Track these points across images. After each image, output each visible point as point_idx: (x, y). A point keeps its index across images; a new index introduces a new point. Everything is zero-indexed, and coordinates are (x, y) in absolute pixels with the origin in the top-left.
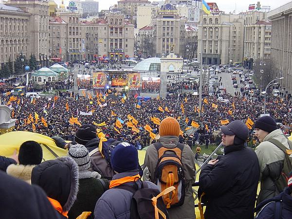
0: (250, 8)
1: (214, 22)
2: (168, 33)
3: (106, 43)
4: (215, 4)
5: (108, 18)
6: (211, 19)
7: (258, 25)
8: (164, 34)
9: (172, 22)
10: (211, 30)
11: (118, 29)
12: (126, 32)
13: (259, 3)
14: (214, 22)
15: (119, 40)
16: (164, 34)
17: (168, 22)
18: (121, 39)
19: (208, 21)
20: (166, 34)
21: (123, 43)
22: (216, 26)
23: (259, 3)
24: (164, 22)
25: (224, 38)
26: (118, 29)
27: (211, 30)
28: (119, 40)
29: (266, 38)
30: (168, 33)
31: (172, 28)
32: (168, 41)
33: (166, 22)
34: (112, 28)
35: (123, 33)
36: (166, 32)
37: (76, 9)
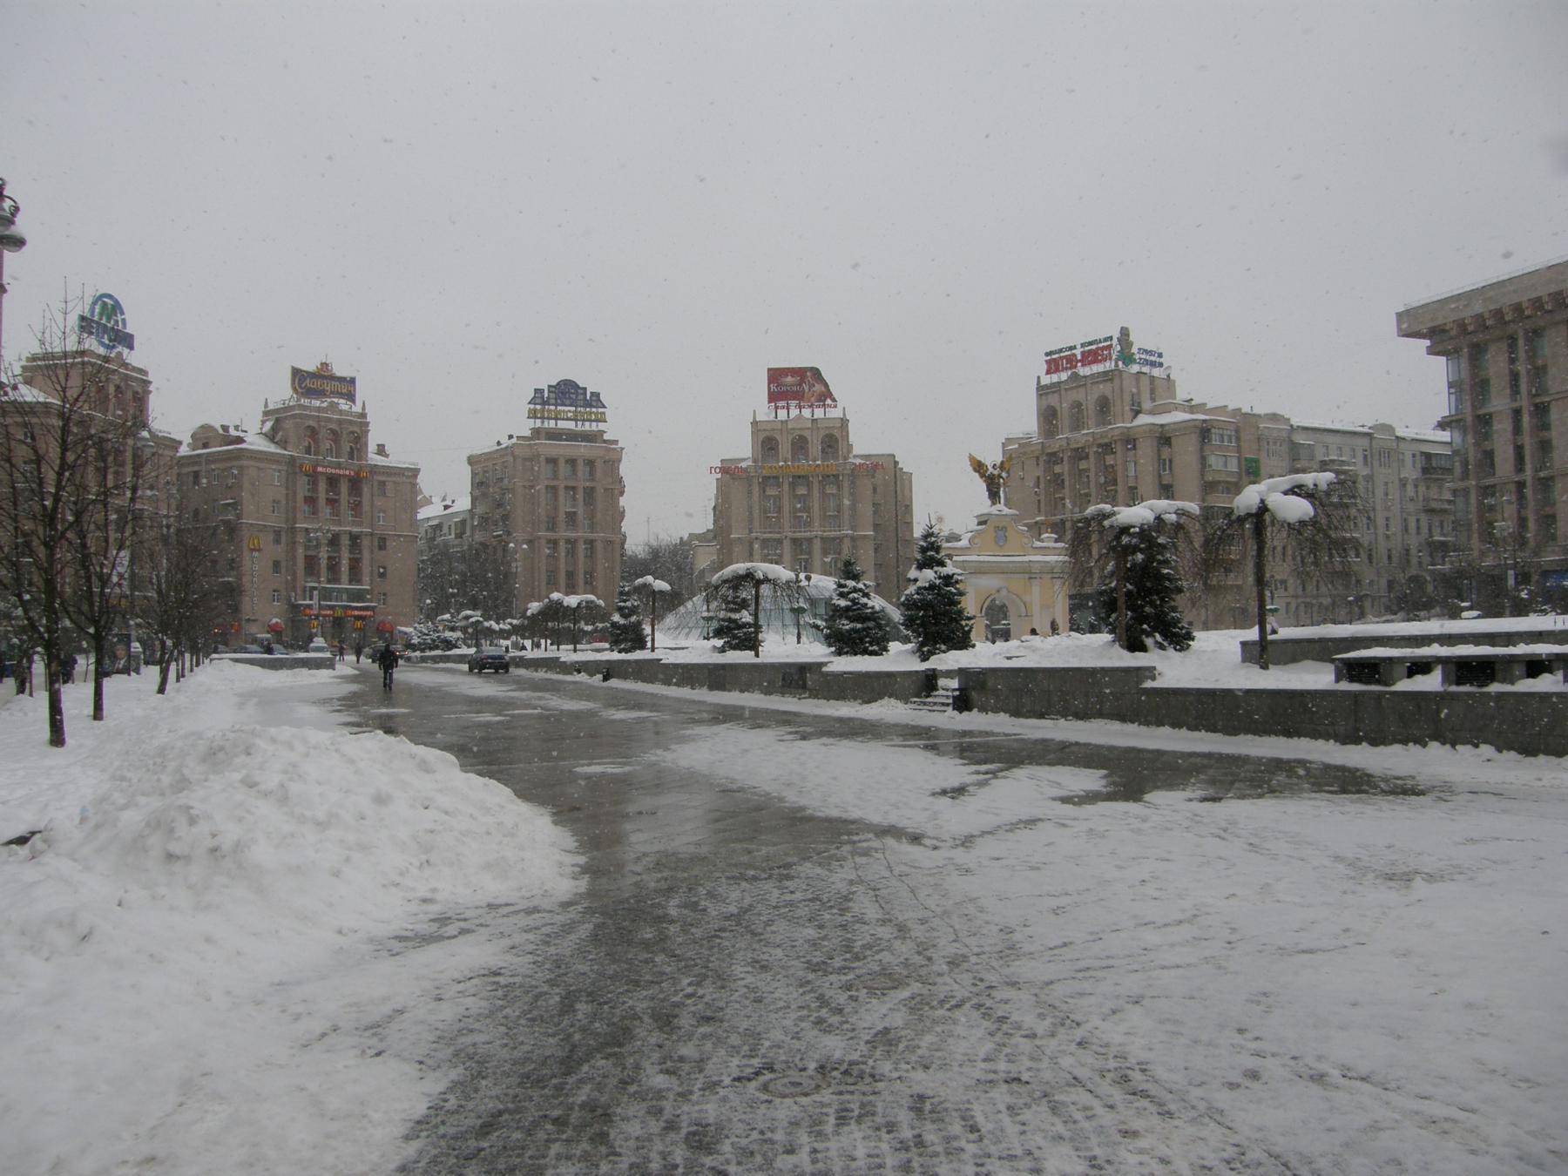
0: (1053, 366)
1: (815, 448)
2: (571, 517)
3: (279, 551)
4: (816, 372)
5: (288, 425)
6: (800, 445)
11: (344, 488)
12: (379, 502)
13: (1125, 332)
15: (345, 541)
18: (355, 539)
19: (785, 448)
20: (562, 517)
21: (366, 555)
23: (1125, 332)
24: (552, 461)
26: (344, 488)
27: (802, 491)
28: (345, 541)
30: (571, 517)
32: (572, 552)
33: (562, 463)
34: (313, 477)
35: (366, 506)
36: (565, 506)
37: (128, 341)
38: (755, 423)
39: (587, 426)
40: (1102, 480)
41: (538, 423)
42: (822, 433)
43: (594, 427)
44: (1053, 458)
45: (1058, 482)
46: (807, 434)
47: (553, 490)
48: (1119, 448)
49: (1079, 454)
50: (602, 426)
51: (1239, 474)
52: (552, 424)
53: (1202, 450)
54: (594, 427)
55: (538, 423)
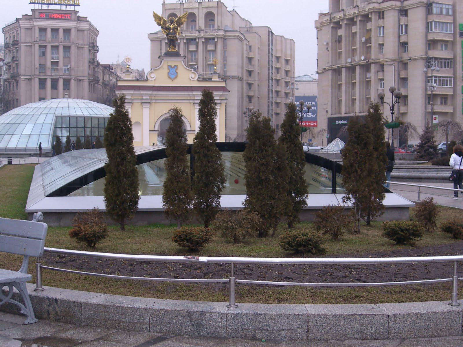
1: (200, 22)
2: (55, 64)
7: (398, 4)
8: (42, 67)
9: (67, 31)
10: (192, 48)
14: (200, 22)
16: (42, 67)
17: (55, 30)
20: (49, 65)
22: (211, 34)
24: (43, 30)
25: (234, 70)
29: (432, 44)
30: (55, 64)
31: (67, 49)
38: (164, 5)
39: (68, 8)
40: (363, 40)
41: (37, 7)
42: (205, 11)
43: (72, 8)
44: (337, 25)
45: (339, 40)
46: (196, 12)
47: (43, 47)
48: (373, 17)
49: (352, 21)
50: (77, 8)
51: (454, 34)
52: (45, 7)
53: (427, 18)
54: (72, 8)
55: (37, 7)
